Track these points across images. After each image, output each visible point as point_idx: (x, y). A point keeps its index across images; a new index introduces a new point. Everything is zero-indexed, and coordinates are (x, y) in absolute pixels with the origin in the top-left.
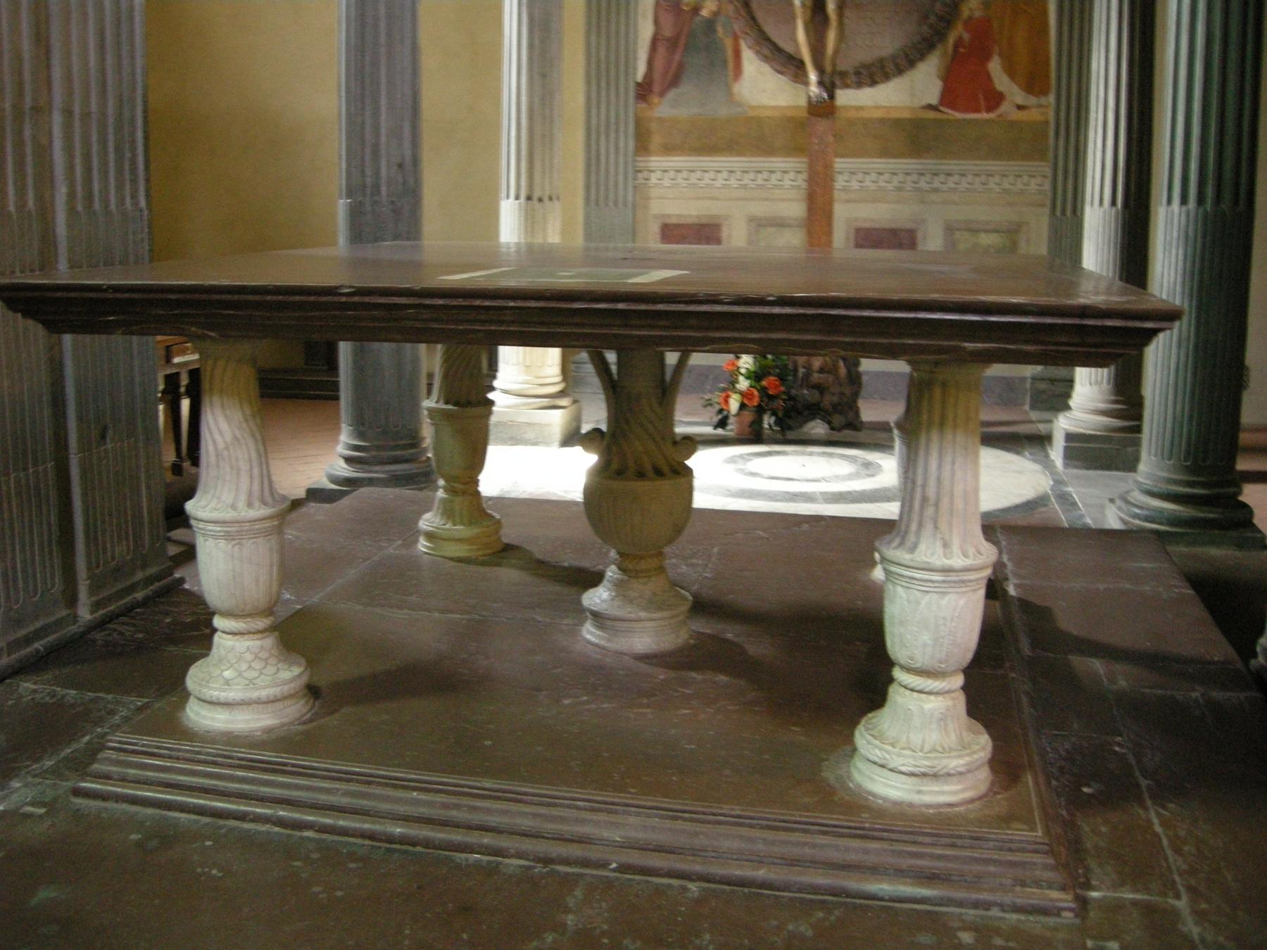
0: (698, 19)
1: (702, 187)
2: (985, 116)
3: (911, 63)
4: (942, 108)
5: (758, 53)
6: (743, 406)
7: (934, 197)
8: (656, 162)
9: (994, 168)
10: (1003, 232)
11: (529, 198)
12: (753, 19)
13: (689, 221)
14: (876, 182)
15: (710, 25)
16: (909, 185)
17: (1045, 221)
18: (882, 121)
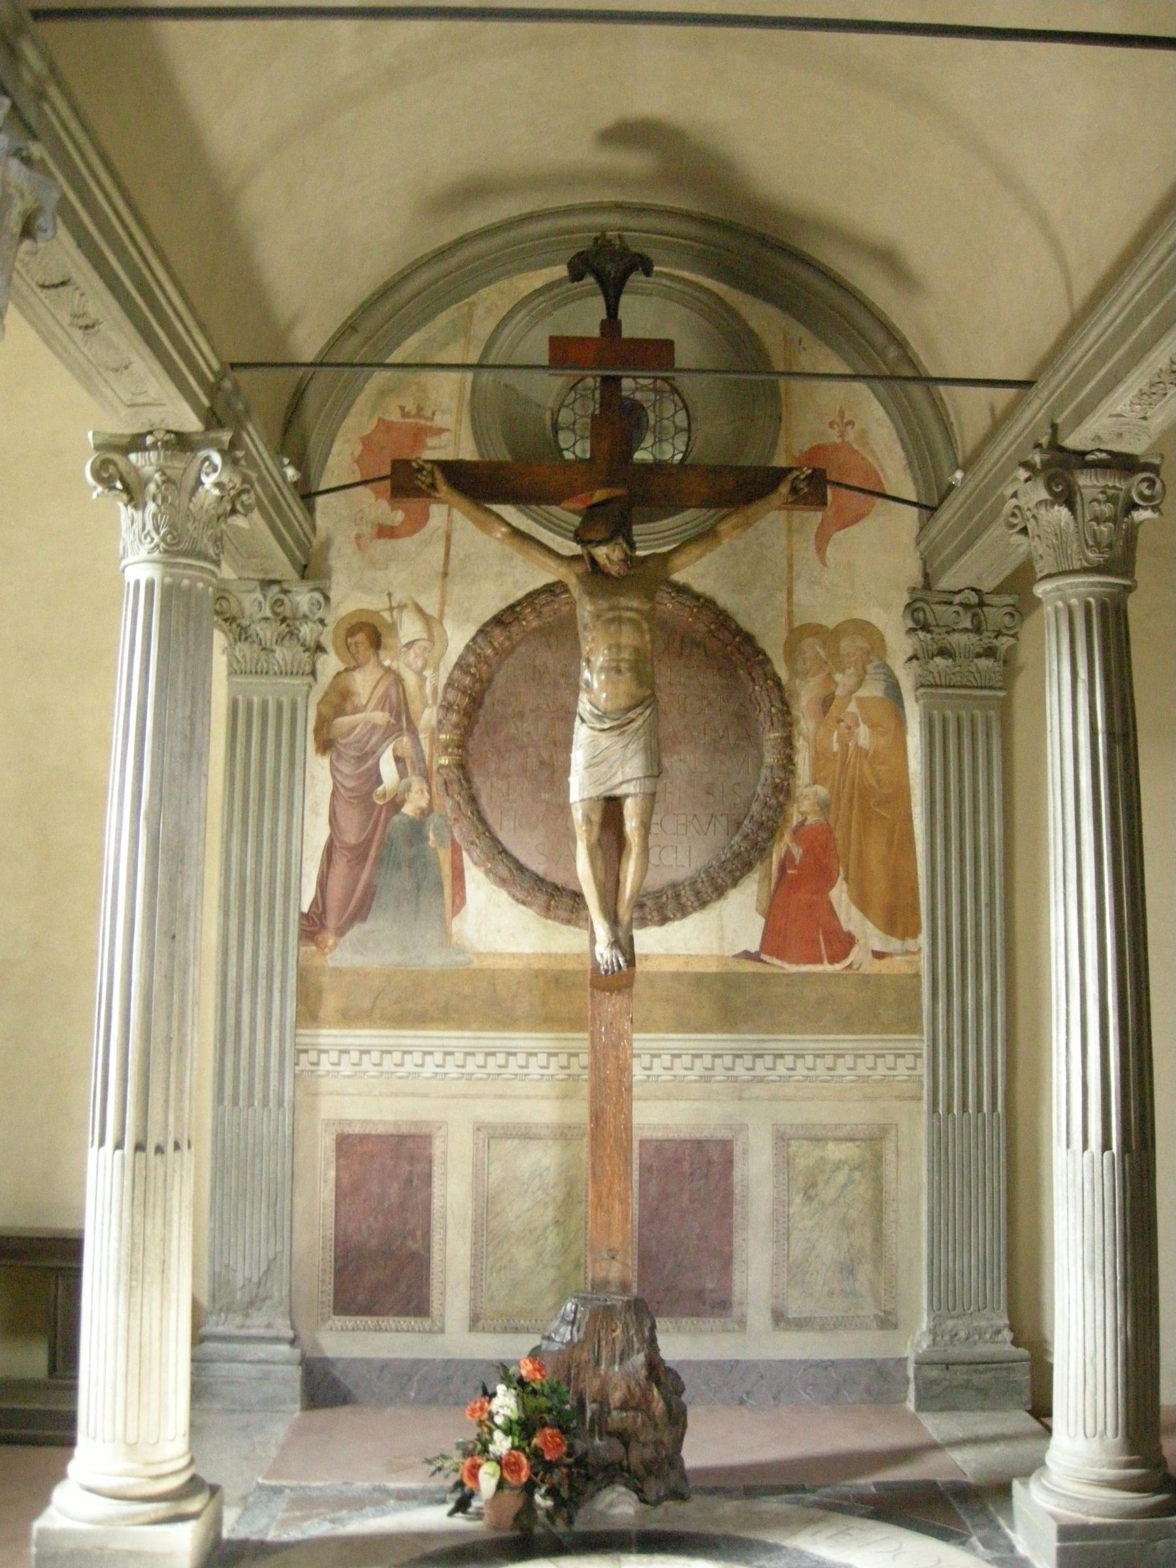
0: (396, 819)
1: (400, 1078)
2: (826, 968)
3: (720, 892)
4: (764, 957)
5: (488, 872)
6: (501, 1485)
7: (758, 1090)
8: (329, 1036)
9: (845, 1045)
10: (862, 1140)
11: (140, 1147)
12: (483, 820)
13: (381, 1130)
14: (670, 1069)
15: (416, 830)
16: (719, 1073)
17: (924, 1120)
18: (677, 976)
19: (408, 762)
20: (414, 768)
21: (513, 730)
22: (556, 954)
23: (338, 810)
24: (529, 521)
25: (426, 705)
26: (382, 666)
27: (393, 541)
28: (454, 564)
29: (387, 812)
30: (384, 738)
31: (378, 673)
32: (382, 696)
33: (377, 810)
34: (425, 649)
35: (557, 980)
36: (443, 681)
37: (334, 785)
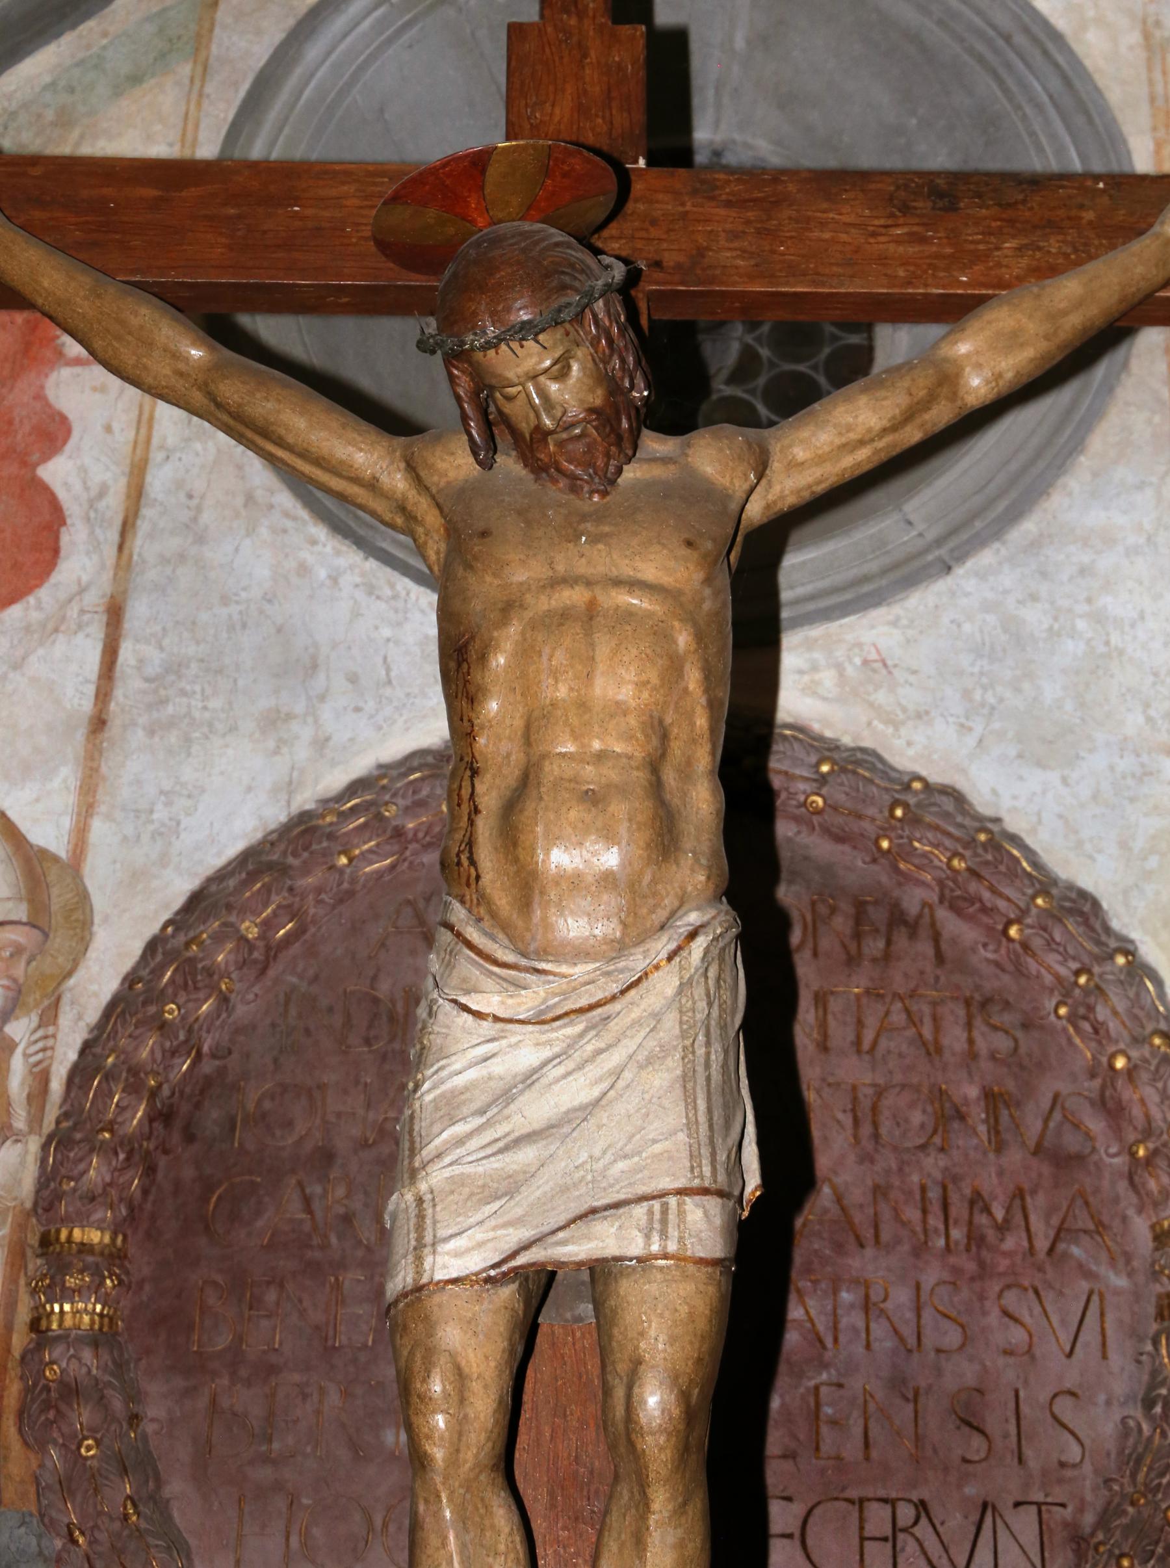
21: (294, 1208)
24: (372, 564)
36: (67, 1054)
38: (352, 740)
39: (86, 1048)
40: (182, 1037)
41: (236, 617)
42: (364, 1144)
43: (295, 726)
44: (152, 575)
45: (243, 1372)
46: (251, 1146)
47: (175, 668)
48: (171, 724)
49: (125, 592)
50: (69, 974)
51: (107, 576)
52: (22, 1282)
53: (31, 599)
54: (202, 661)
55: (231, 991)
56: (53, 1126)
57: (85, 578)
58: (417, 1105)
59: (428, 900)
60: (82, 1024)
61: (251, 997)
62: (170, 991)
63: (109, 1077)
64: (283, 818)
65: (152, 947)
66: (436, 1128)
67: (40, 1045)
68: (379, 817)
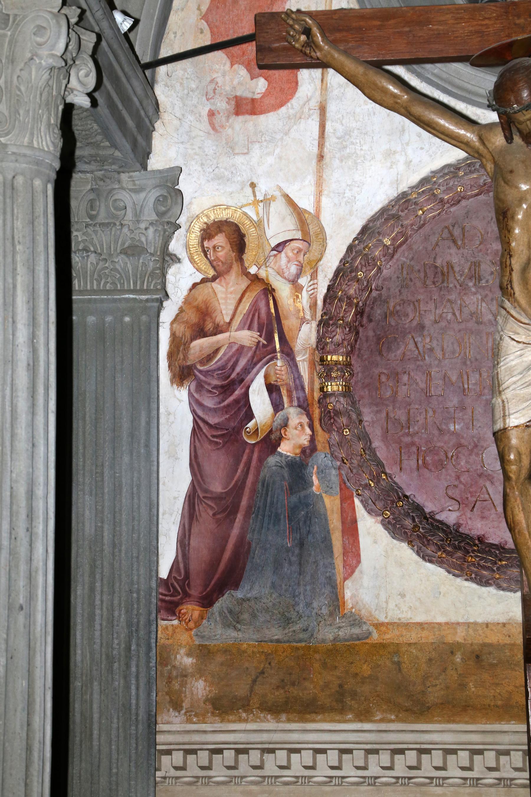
0: (272, 460)
19: (284, 392)
20: (290, 396)
21: (411, 346)
22: (475, 624)
23: (200, 452)
25: (303, 321)
26: (247, 274)
27: (254, 117)
28: (331, 142)
29: (260, 451)
30: (252, 364)
31: (244, 283)
32: (249, 311)
33: (247, 451)
34: (300, 251)
35: (478, 657)
36: (322, 291)
37: (195, 421)
38: (420, 161)
39: (329, 288)
40: (365, 283)
41: (371, 110)
42: (436, 322)
43: (397, 156)
44: (336, 92)
45: (397, 405)
46: (393, 323)
47: (348, 133)
48: (349, 156)
49: (326, 100)
50: (320, 260)
51: (318, 93)
52: (315, 374)
53: (289, 104)
54: (358, 129)
55: (381, 265)
56: (320, 318)
57: (309, 94)
58: (499, 370)
59: (453, 226)
60: (327, 279)
61: (388, 266)
62: (360, 267)
63: (340, 300)
64: (396, 195)
65: (350, 248)
66: (506, 378)
67: (312, 287)
68: (434, 195)
